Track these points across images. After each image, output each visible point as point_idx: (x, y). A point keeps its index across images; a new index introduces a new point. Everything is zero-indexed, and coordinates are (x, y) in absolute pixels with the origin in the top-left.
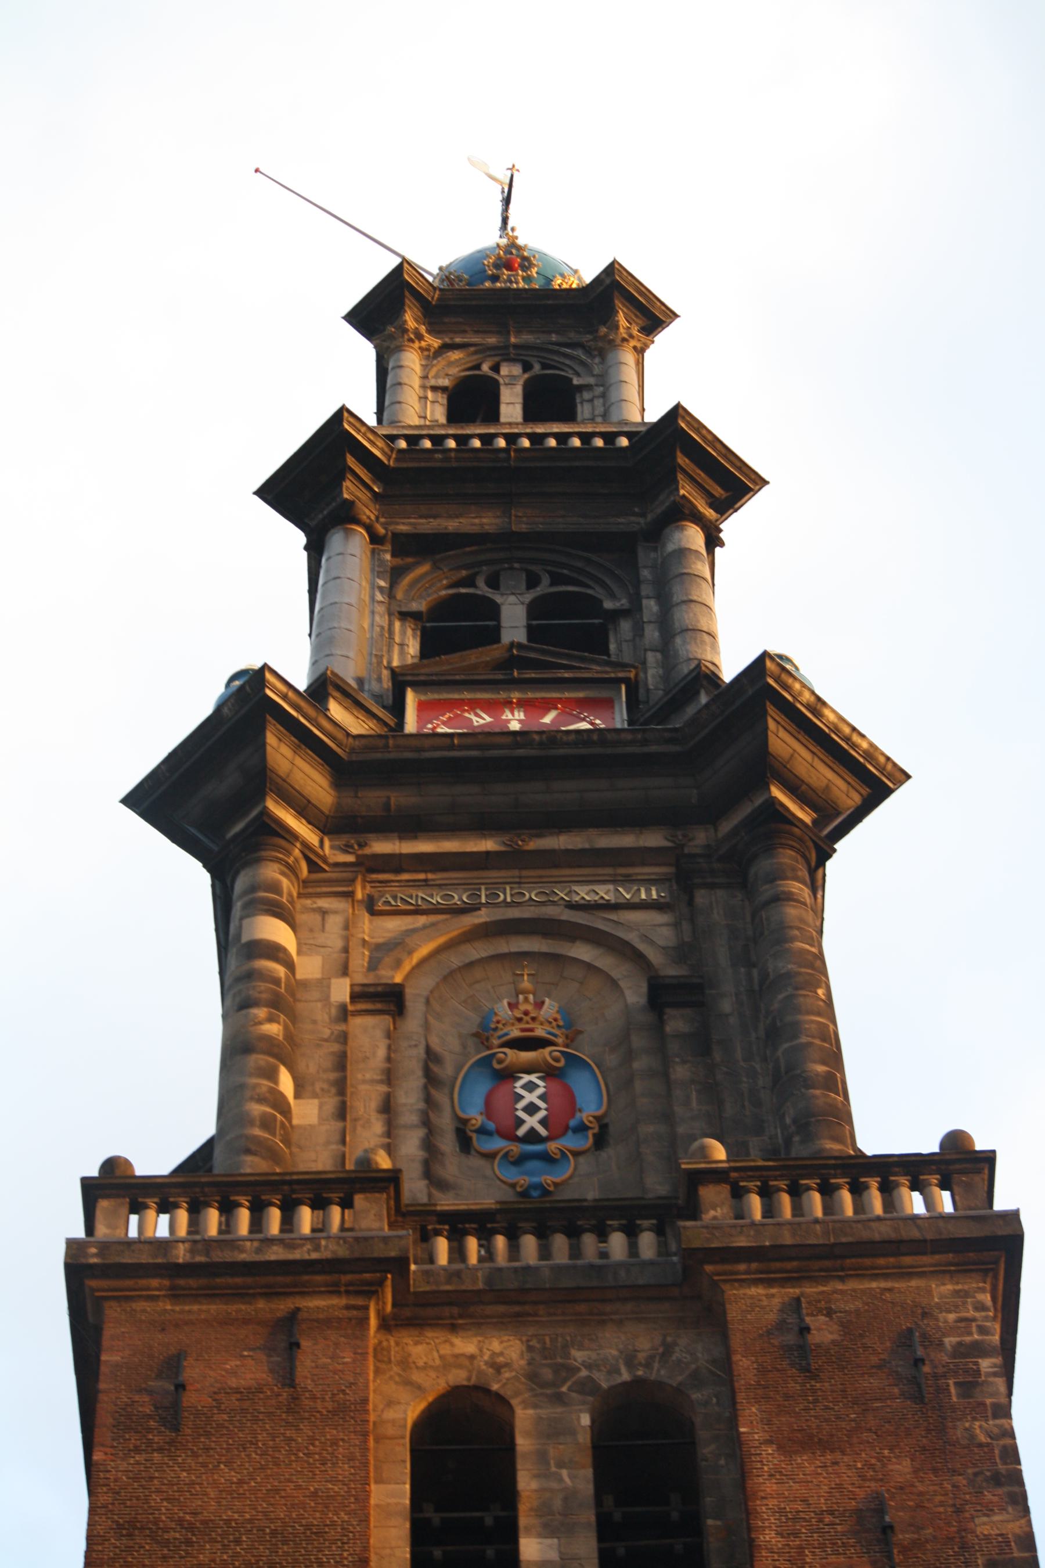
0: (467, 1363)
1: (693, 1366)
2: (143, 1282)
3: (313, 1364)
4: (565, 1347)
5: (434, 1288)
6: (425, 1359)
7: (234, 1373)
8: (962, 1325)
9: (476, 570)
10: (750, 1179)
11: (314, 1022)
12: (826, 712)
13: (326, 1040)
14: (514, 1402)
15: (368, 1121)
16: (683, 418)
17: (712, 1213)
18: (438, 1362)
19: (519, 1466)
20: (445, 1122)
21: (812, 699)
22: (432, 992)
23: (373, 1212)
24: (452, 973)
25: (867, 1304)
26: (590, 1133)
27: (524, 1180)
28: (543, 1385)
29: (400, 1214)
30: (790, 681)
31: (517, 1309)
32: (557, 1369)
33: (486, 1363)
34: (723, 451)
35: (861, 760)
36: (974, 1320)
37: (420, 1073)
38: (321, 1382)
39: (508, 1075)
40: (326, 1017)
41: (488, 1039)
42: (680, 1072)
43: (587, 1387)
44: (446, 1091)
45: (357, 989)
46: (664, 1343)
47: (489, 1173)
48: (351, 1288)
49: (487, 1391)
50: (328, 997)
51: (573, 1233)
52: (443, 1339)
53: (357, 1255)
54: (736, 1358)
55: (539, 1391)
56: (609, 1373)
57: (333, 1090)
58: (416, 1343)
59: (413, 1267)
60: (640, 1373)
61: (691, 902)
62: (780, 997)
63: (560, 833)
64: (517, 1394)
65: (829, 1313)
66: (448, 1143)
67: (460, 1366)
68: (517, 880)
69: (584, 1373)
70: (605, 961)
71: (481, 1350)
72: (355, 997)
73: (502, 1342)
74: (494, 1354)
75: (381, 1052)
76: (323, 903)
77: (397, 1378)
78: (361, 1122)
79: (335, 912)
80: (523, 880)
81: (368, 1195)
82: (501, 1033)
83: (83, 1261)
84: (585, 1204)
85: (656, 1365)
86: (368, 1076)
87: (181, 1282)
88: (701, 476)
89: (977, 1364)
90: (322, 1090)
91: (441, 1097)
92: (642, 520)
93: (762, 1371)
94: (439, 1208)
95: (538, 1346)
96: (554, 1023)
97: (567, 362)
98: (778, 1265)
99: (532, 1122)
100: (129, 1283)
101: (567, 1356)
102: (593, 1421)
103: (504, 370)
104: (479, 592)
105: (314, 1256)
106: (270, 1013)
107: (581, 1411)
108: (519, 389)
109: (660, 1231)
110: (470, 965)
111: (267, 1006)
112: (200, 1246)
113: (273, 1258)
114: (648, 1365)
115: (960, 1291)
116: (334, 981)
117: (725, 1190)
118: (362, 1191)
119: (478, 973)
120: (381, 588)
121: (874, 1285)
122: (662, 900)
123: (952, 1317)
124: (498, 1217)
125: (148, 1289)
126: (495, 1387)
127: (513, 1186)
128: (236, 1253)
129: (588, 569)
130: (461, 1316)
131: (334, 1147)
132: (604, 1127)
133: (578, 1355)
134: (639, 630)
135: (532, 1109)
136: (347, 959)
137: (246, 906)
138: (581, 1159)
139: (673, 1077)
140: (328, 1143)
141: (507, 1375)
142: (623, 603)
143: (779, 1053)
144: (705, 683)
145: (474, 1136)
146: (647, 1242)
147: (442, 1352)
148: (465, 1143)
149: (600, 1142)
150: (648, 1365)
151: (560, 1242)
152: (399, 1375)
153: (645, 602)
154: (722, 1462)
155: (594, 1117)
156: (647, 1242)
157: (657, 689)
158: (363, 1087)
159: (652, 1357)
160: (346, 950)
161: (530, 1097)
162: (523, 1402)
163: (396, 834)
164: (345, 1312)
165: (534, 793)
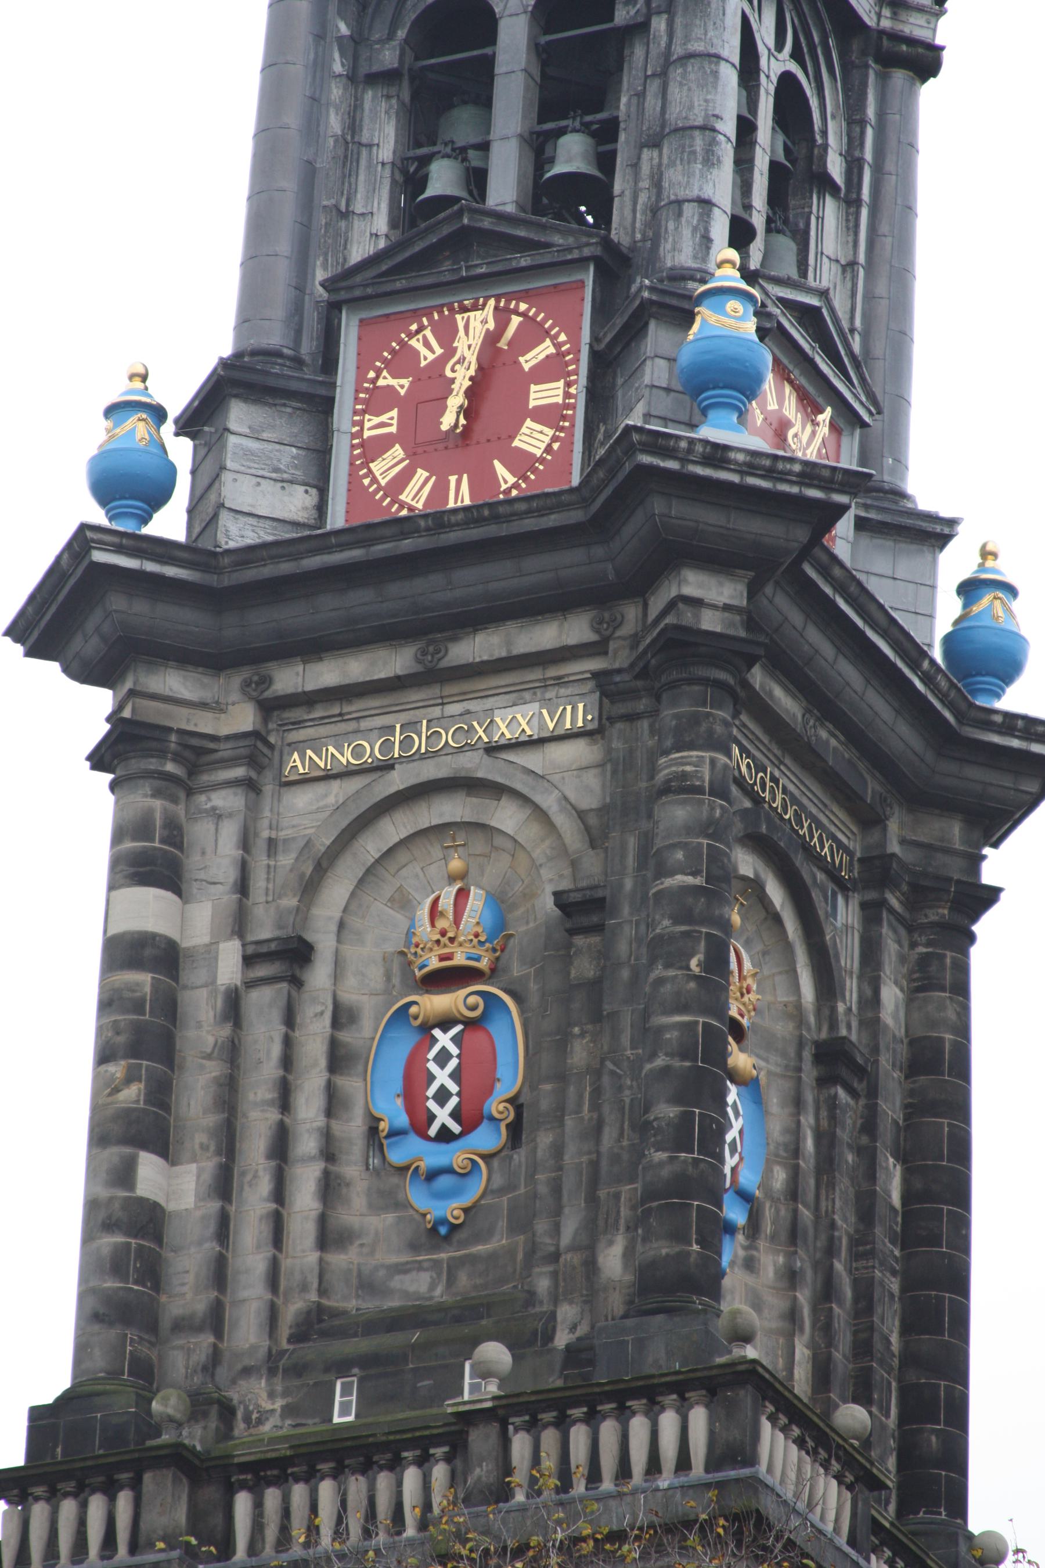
12: (732, 455)
13: (209, 1057)
22: (345, 910)
24: (369, 871)
40: (211, 1014)
50: (214, 982)
63: (476, 631)
68: (440, 701)
72: (249, 961)
75: (276, 1050)
78: (249, 1177)
79: (230, 815)
80: (445, 701)
90: (201, 1145)
91: (350, 1084)
94: (236, 1460)
96: (475, 941)
106: (129, 1068)
110: (390, 852)
111: (126, 1057)
117: (494, 1428)
119: (402, 856)
131: (207, 1245)
135: (443, 1095)
138: (495, 1163)
140: (200, 1243)
155: (507, 1101)
163: (299, 659)
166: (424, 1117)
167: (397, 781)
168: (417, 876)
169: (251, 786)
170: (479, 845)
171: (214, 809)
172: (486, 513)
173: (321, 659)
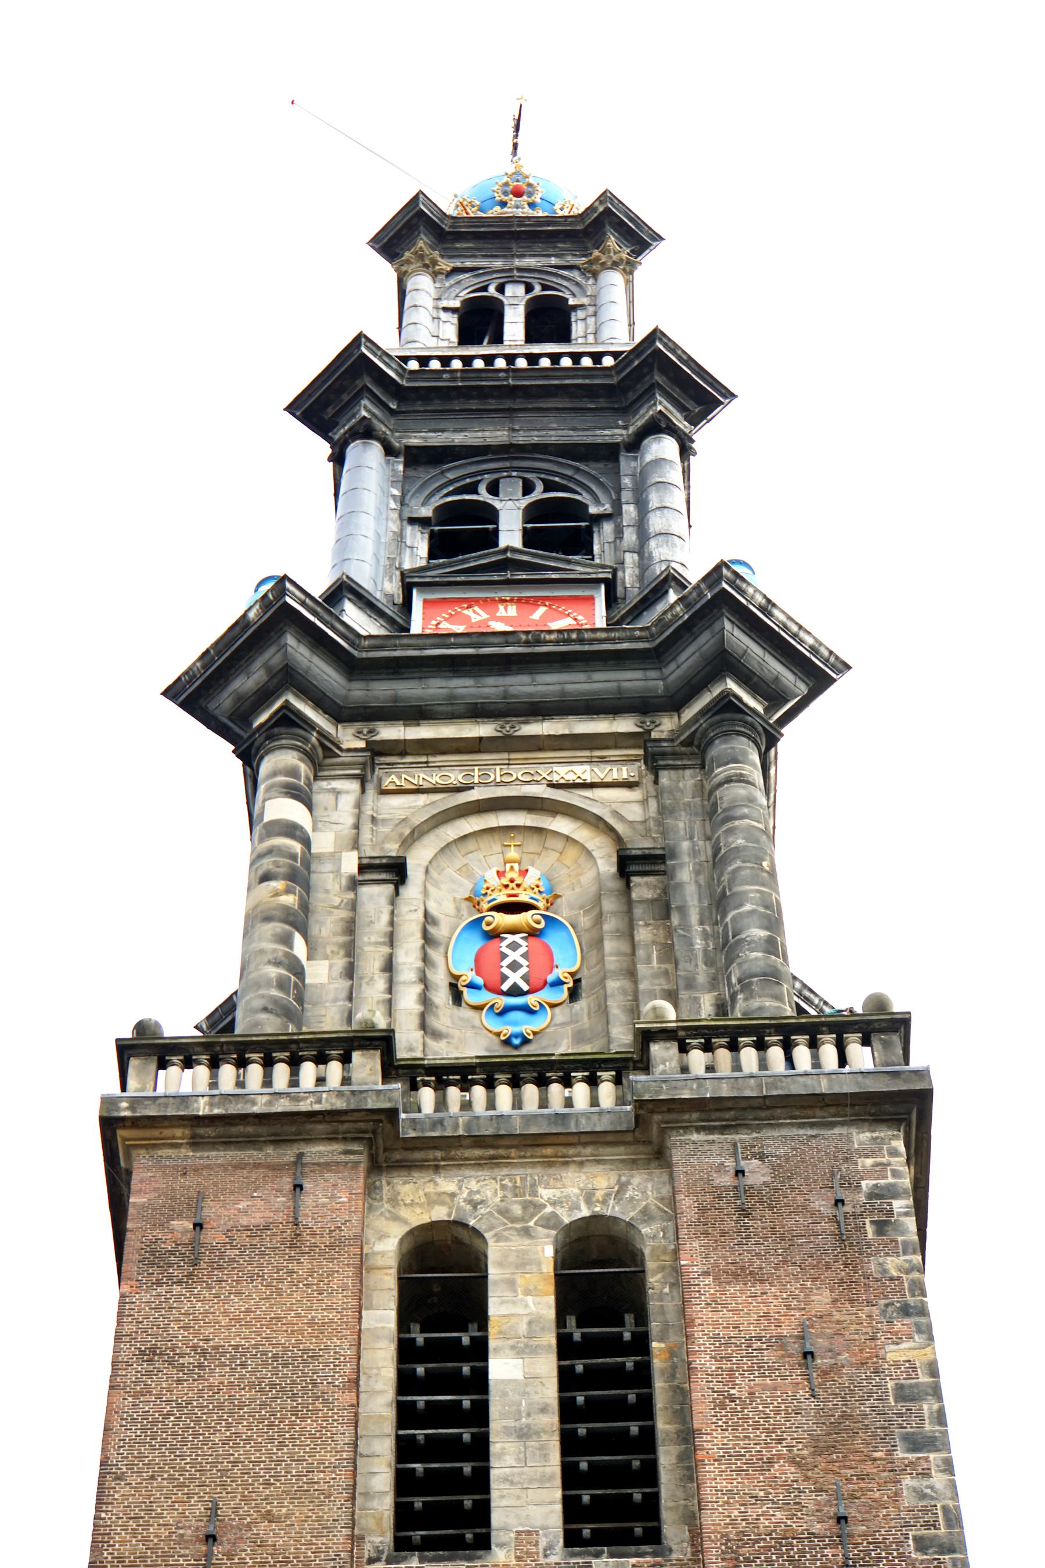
0: (448, 1200)
1: (644, 1203)
2: (167, 1132)
3: (314, 1204)
4: (533, 1185)
5: (421, 1134)
6: (412, 1197)
7: (245, 1212)
8: (877, 1169)
9: (479, 478)
10: (694, 1037)
11: (327, 891)
13: (337, 908)
14: (486, 1235)
15: (372, 979)
16: (661, 340)
17: (661, 1067)
18: (423, 1199)
19: (490, 1294)
20: (440, 979)
21: (764, 601)
22: (430, 862)
23: (369, 1067)
24: (448, 845)
25: (795, 1149)
26: (565, 987)
27: (508, 1030)
28: (514, 1220)
29: (391, 1069)
30: (744, 586)
31: (492, 1152)
32: (526, 1206)
33: (465, 1200)
34: (697, 369)
35: (808, 654)
36: (889, 1164)
37: (418, 935)
38: (319, 1219)
39: (494, 935)
40: (337, 887)
41: (479, 903)
42: (643, 934)
43: (550, 1221)
44: (442, 950)
45: (365, 861)
46: (618, 1182)
47: (477, 1023)
48: (348, 1135)
49: (465, 1226)
51: (542, 1083)
52: (428, 1179)
53: (352, 1107)
54: (680, 1197)
55: (510, 1225)
56: (571, 1209)
57: (342, 952)
58: (405, 1183)
59: (403, 1116)
60: (597, 1209)
61: (656, 782)
62: (730, 869)
64: (491, 1228)
65: (762, 1157)
66: (441, 996)
67: (442, 1203)
69: (549, 1209)
70: (581, 833)
71: (460, 1188)
72: (362, 868)
73: (478, 1182)
74: (471, 1193)
75: (385, 918)
76: (336, 784)
77: (387, 1215)
78: (366, 980)
79: (347, 792)
81: (365, 1052)
82: (489, 898)
83: (115, 1114)
84: (553, 1058)
85: (611, 1202)
86: (373, 939)
87: (201, 1131)
88: (676, 392)
89: (890, 1204)
90: (332, 952)
91: (435, 955)
92: (624, 432)
93: (703, 1210)
95: (510, 1184)
96: (536, 890)
97: (565, 283)
98: (718, 1114)
99: (515, 978)
100: (156, 1133)
101: (534, 1193)
102: (556, 1252)
103: (509, 290)
104: (481, 499)
105: (317, 1107)
106: (287, 886)
107: (546, 1244)
108: (521, 310)
109: (618, 1081)
110: (465, 838)
111: (284, 879)
112: (217, 1099)
113: (280, 1110)
114: (604, 1202)
115: (877, 1138)
116: (344, 854)
118: (360, 1048)
119: (471, 844)
120: (394, 496)
121: (801, 1132)
122: (631, 779)
123: (869, 1162)
124: (478, 1070)
125: (174, 1138)
126: (472, 1222)
127: (498, 1034)
128: (248, 1106)
129: (576, 477)
130: (443, 1159)
132: (577, 982)
133: (545, 1194)
134: (619, 533)
135: (514, 966)
136: (358, 834)
137: (268, 790)
138: (557, 1010)
139: (637, 938)
140: (335, 1000)
141: (482, 1211)
142: (607, 508)
143: (728, 919)
144: (673, 584)
145: (465, 990)
146: (607, 1090)
147: (427, 1190)
148: (457, 997)
149: (574, 994)
150: (604, 1202)
151: (530, 1091)
152: (390, 1212)
153: (625, 507)
154: (667, 1290)
156: (607, 1090)
157: (633, 587)
158: (367, 949)
159: (608, 1195)
160: (357, 826)
161: (514, 956)
162: (496, 1235)
164: (343, 1157)
165: (522, 685)
166: (497, 978)
167: (475, 795)
168: (480, 860)
169: (363, 780)
170: (533, 844)
171: (334, 789)
172: (574, 636)
173: (418, 725)
